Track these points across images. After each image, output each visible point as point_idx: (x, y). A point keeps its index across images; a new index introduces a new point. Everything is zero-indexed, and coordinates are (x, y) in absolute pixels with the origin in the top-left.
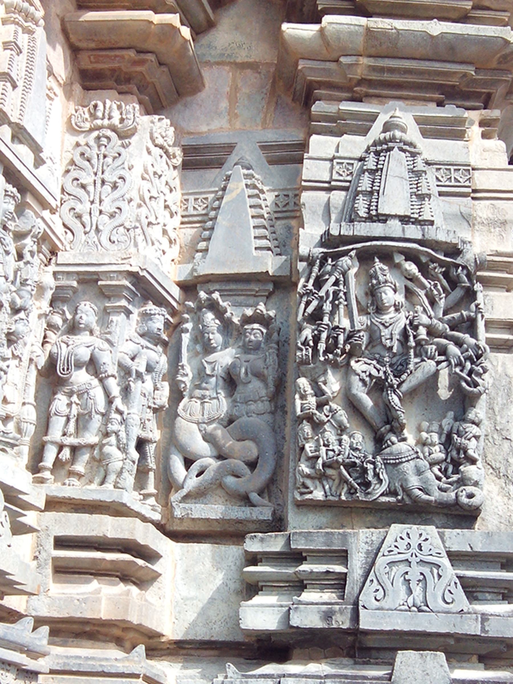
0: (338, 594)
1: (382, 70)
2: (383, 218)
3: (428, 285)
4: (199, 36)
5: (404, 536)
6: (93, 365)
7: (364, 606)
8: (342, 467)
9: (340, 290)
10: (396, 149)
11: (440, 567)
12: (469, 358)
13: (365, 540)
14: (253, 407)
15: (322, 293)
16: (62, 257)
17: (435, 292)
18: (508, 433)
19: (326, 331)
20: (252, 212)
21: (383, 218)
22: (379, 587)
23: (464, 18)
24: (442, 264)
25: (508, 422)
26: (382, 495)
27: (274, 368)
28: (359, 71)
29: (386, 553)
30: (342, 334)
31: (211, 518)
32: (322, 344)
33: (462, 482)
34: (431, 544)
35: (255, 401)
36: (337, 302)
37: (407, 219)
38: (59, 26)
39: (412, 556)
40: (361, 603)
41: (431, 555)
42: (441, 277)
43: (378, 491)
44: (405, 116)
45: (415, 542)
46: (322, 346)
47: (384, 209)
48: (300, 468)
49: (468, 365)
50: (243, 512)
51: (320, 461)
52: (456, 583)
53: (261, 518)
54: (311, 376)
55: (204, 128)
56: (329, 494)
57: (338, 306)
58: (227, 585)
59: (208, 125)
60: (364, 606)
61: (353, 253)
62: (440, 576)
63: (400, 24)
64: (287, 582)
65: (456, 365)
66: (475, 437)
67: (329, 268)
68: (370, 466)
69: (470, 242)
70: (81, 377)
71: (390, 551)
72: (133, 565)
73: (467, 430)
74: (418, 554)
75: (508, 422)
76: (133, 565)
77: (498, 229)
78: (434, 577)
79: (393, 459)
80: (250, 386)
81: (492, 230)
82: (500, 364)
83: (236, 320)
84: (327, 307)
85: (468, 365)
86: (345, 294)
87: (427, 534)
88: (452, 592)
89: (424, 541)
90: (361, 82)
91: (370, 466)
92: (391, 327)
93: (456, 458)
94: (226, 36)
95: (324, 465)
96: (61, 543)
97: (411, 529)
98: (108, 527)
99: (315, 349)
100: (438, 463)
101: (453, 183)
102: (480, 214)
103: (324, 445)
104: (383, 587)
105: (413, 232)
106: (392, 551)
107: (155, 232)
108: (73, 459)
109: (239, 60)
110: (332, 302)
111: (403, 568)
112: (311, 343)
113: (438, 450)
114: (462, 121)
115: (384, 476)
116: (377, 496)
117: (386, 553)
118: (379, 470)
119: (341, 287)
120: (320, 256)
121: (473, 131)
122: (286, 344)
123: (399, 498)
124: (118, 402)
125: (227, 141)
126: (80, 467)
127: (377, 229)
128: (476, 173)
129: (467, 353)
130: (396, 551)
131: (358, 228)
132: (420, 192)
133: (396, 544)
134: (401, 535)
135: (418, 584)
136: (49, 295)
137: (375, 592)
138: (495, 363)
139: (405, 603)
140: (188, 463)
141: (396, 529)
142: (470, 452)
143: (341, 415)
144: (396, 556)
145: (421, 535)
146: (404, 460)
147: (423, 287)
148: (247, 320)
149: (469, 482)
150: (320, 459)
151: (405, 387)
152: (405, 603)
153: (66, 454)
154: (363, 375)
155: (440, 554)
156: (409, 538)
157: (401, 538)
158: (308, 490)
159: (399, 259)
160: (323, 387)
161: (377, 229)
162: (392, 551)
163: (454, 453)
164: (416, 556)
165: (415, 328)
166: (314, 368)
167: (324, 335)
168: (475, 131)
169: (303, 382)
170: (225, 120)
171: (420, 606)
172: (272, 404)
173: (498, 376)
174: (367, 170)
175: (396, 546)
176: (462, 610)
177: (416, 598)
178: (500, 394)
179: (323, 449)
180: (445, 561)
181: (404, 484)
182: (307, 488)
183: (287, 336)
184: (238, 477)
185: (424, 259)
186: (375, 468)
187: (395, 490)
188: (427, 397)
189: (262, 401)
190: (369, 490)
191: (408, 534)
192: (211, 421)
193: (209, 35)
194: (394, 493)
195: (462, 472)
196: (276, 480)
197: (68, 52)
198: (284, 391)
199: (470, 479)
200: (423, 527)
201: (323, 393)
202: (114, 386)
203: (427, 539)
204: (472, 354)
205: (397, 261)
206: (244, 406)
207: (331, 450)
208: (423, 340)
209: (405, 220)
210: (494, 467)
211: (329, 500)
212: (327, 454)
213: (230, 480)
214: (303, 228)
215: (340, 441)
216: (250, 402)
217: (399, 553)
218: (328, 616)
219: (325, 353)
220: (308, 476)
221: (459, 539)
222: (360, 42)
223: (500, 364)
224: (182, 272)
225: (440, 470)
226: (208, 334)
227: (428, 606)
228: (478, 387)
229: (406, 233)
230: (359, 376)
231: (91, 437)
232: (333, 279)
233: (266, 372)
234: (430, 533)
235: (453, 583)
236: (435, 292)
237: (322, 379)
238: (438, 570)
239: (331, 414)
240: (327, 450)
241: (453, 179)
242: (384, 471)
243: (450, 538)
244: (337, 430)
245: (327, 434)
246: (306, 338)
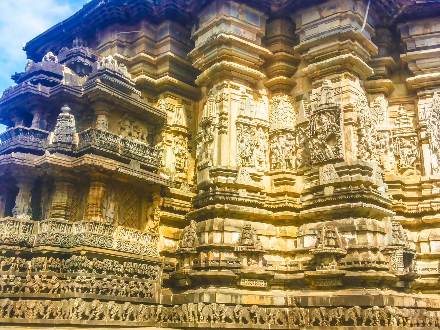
1: (322, 72)
6: (277, 148)
16: (270, 130)
23: (338, 54)
24: (333, 111)
38: (167, 154)
44: (327, 81)
63: (322, 62)
70: (276, 151)
72: (291, 182)
76: (291, 182)
83: (304, 131)
90: (320, 75)
93: (337, 150)
96: (275, 180)
98: (281, 176)
100: (335, 151)
105: (327, 106)
107: (289, 119)
108: (276, 166)
114: (340, 77)
124: (281, 154)
126: (278, 167)
127: (321, 108)
136: (268, 137)
153: (275, 165)
159: (326, 112)
161: (321, 108)
169: (310, 142)
197: (267, 89)
202: (281, 151)
209: (325, 104)
218: (316, 184)
222: (316, 68)
224: (295, 125)
231: (278, 161)
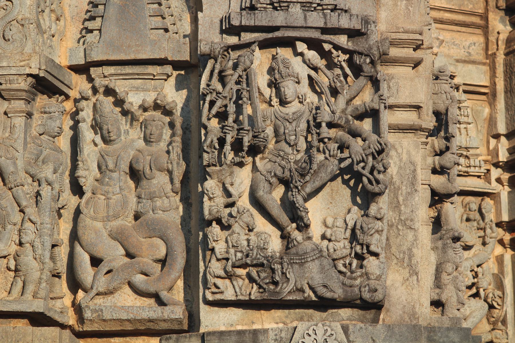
5: (311, 332)
9: (243, 89)
13: (274, 337)
17: (338, 84)
18: (412, 223)
24: (345, 51)
25: (412, 211)
26: (290, 292)
36: (240, 102)
37: (308, 5)
42: (344, 65)
50: (155, 311)
53: (173, 316)
54: (218, 178)
56: (239, 293)
66: (377, 231)
69: (374, 22)
75: (412, 211)
79: (299, 259)
81: (399, 3)
82: (405, 151)
87: (332, 330)
95: (234, 266)
103: (233, 246)
113: (342, 246)
118: (286, 270)
119: (245, 86)
131: (260, 17)
134: (307, 332)
138: (400, 151)
140: (96, 262)
142: (373, 248)
150: (230, 261)
156: (316, 334)
158: (220, 290)
159: (301, 47)
173: (402, 164)
178: (404, 183)
184: (146, 275)
187: (302, 288)
188: (332, 190)
204: (374, 151)
207: (239, 251)
212: (236, 255)
214: (202, 11)
223: (405, 151)
225: (345, 265)
228: (379, 185)
229: (308, 21)
234: (335, 328)
236: (338, 84)
240: (236, 251)
242: (291, 270)
243: (354, 332)
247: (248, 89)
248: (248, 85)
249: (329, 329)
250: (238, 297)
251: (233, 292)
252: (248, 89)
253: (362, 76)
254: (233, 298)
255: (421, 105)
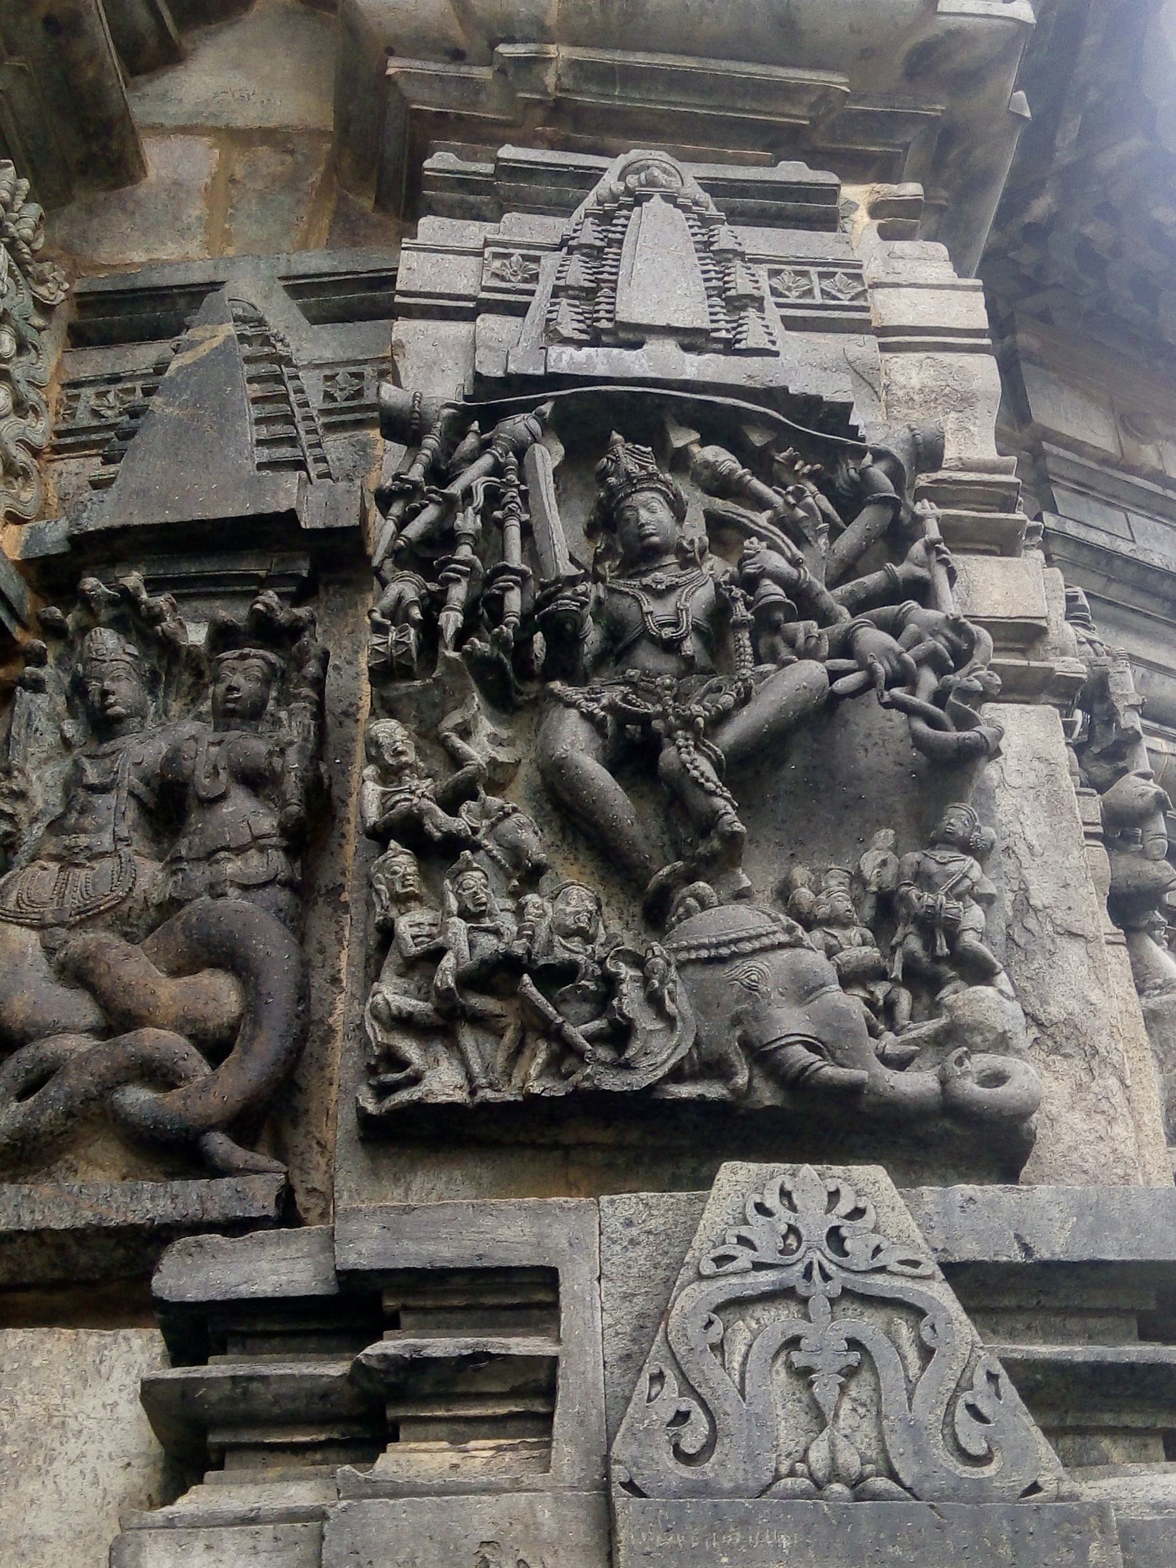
0: (525, 1453)
2: (633, 336)
3: (778, 500)
4: (141, 79)
5: (772, 1201)
7: (630, 1486)
8: (526, 978)
10: (657, 198)
11: (920, 1313)
12: (933, 660)
14: (231, 867)
15: (456, 489)
19: (464, 582)
20: (256, 390)
21: (633, 336)
22: (689, 1404)
26: (677, 1075)
27: (302, 750)
28: (550, 80)
29: (708, 1268)
30: (517, 590)
31: (55, 1225)
32: (451, 613)
33: (951, 1036)
34: (875, 1230)
35: (240, 850)
36: (498, 514)
39: (807, 1274)
40: (619, 1473)
41: (882, 1270)
43: (657, 1053)
45: (815, 1222)
46: (451, 621)
47: (634, 307)
48: (379, 997)
49: (929, 679)
50: (174, 1198)
51: (448, 962)
52: (992, 1377)
55: (139, 256)
57: (501, 525)
58: (96, 1482)
59: (147, 251)
60: (630, 1486)
61: (547, 408)
62: (927, 1353)
64: (321, 1422)
65: (891, 683)
67: (471, 441)
68: (626, 971)
71: (721, 1260)
73: (952, 867)
74: (831, 1269)
77: (953, 415)
78: (903, 1358)
80: (226, 809)
84: (468, 522)
85: (929, 679)
86: (524, 495)
87: (859, 1193)
88: (985, 1411)
89: (849, 1216)
91: (626, 971)
92: (672, 599)
94: (207, 79)
97: (793, 1175)
99: (430, 631)
101: (819, 300)
102: (902, 380)
103: (464, 914)
104: (703, 1404)
106: (732, 1258)
109: (240, 122)
110: (484, 513)
111: (779, 1320)
112: (416, 613)
113: (858, 939)
115: (680, 1003)
116: (660, 1073)
117: (708, 1268)
120: (447, 412)
121: (854, 222)
122: (347, 722)
123: (741, 1080)
125: (198, 277)
128: (879, 295)
129: (922, 646)
130: (745, 1257)
132: (732, 293)
133: (744, 1231)
135: (843, 1388)
137: (671, 1423)
139: (800, 1467)
141: (736, 1178)
142: (970, 939)
143: (521, 826)
144: (750, 1279)
145: (834, 1196)
146: (747, 947)
147: (761, 504)
148: (223, 636)
149: (978, 1039)
151: (730, 734)
152: (800, 1467)
154: (593, 706)
155: (915, 1264)
156: (793, 1208)
157: (761, 1208)
160: (459, 743)
162: (732, 1258)
163: (914, 944)
164: (826, 1277)
165: (750, 583)
166: (425, 689)
167: (458, 593)
168: (862, 223)
170: (196, 243)
171: (862, 1478)
172: (298, 865)
174: (580, 247)
175: (743, 1241)
176: (1035, 1488)
177: (841, 1443)
179: (459, 926)
180: (941, 1295)
181: (755, 1031)
182: (404, 1064)
183: (352, 699)
185: (757, 439)
186: (646, 981)
189: (262, 850)
190: (630, 1053)
191: (785, 1194)
192: (87, 918)
193: (165, 79)
194: (716, 1068)
195: (950, 1008)
196: (307, 1111)
198: (341, 846)
199: (976, 1028)
200: (837, 1170)
201: (456, 760)
203: (857, 1213)
205: (678, 443)
206: (204, 866)
207: (487, 930)
208: (777, 605)
209: (692, 340)
210: (1042, 1017)
211: (486, 1105)
212: (472, 945)
213: (137, 1098)
215: (519, 912)
216: (222, 854)
217: (758, 1266)
219: (461, 637)
220: (404, 1023)
221: (982, 1217)
226: (101, 680)
227: (893, 1476)
230: (578, 707)
232: (486, 461)
233: (277, 762)
235: (980, 1379)
237: (455, 718)
238: (915, 1327)
239: (485, 822)
241: (817, 292)
244: (509, 878)
245: (473, 879)
246: (400, 599)
247: (523, 487)
248: (523, 481)
249: (846, 1192)
250: (481, 1093)
251: (460, 1079)
252: (523, 487)
253: (870, 503)
254: (460, 1097)
255: (1043, 623)
